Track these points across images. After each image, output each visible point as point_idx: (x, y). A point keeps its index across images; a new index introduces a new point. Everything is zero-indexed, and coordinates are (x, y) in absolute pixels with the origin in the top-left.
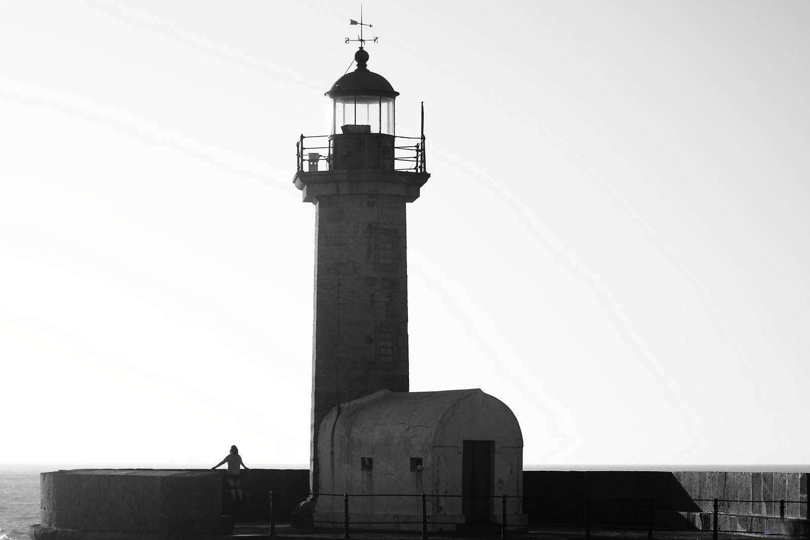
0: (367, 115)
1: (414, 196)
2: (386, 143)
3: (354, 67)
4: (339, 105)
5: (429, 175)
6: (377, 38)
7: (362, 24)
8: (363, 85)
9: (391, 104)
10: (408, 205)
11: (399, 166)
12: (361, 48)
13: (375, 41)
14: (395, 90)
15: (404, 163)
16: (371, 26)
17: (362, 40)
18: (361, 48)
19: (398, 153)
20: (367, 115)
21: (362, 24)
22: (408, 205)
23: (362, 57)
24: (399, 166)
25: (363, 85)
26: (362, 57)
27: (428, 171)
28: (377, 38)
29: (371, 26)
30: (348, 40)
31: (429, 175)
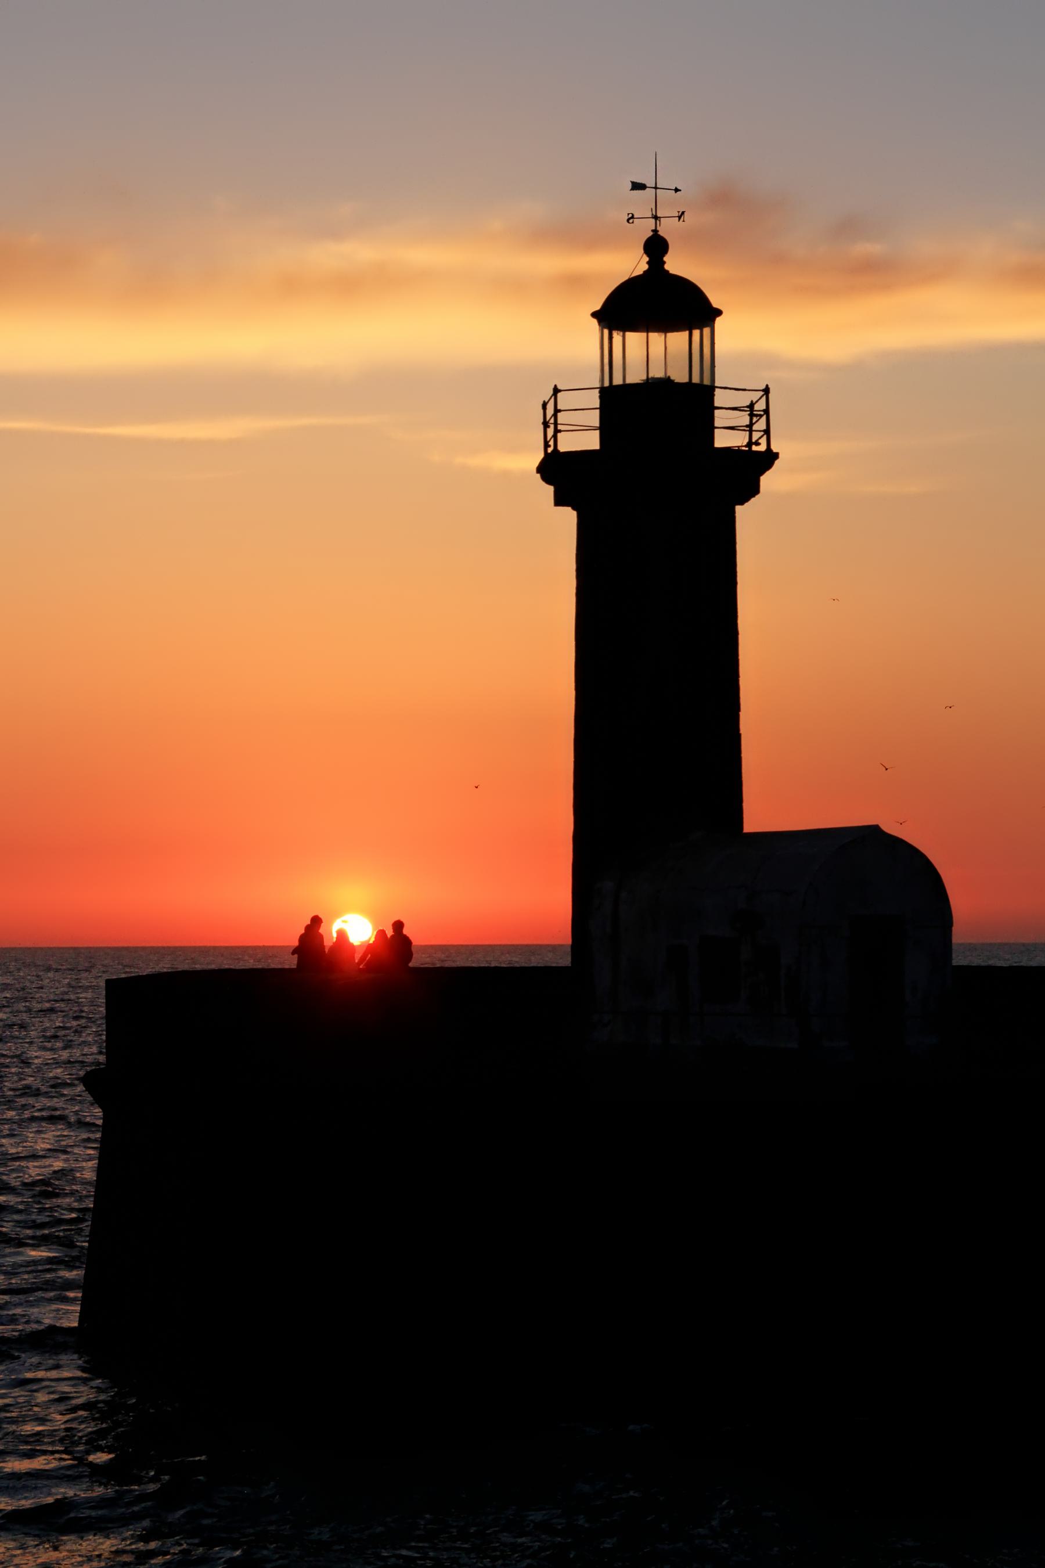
0: (651, 354)
2: (694, 400)
3: (640, 265)
4: (617, 337)
5: (776, 456)
6: (683, 213)
7: (656, 188)
8: (656, 299)
9: (707, 331)
10: (738, 508)
11: (723, 440)
12: (655, 231)
13: (680, 217)
14: (715, 305)
16: (677, 190)
17: (656, 218)
18: (655, 231)
19: (721, 418)
20: (651, 354)
21: (656, 188)
22: (741, 512)
23: (656, 247)
24: (723, 440)
26: (656, 247)
27: (775, 448)
28: (683, 213)
29: (677, 190)
30: (633, 217)
31: (776, 456)
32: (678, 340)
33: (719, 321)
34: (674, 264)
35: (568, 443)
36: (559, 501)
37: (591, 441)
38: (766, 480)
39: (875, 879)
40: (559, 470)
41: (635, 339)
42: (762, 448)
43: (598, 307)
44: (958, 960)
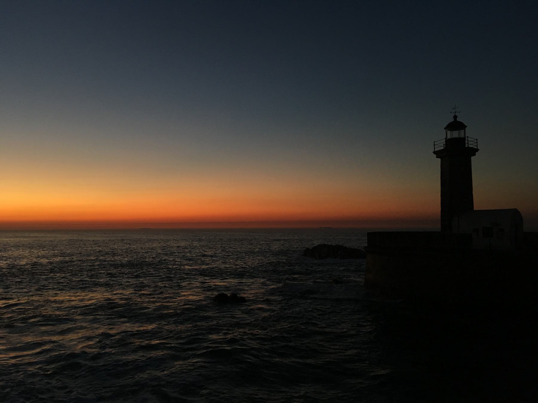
1: (475, 155)
2: (462, 140)
8: (456, 125)
15: (471, 145)
23: (455, 117)
25: (456, 125)
26: (455, 117)
33: (466, 129)
34: (458, 120)
38: (477, 153)
42: (476, 147)
43: (445, 126)
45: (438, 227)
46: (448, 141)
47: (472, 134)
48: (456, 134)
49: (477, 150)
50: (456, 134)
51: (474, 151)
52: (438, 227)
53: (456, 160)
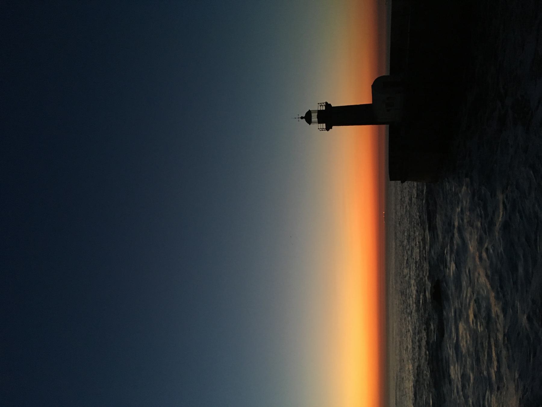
1: (330, 104)
2: (319, 112)
8: (308, 118)
11: (324, 108)
22: (333, 105)
23: (302, 118)
24: (324, 108)
25: (308, 118)
26: (302, 118)
32: (313, 114)
34: (304, 116)
35: (325, 127)
36: (331, 128)
37: (324, 124)
38: (329, 103)
39: (378, 86)
40: (328, 128)
41: (313, 120)
44: (389, 74)
45: (384, 128)
46: (320, 122)
47: (315, 107)
48: (314, 118)
49: (326, 103)
50: (314, 118)
51: (328, 105)
52: (384, 128)
53: (333, 116)
